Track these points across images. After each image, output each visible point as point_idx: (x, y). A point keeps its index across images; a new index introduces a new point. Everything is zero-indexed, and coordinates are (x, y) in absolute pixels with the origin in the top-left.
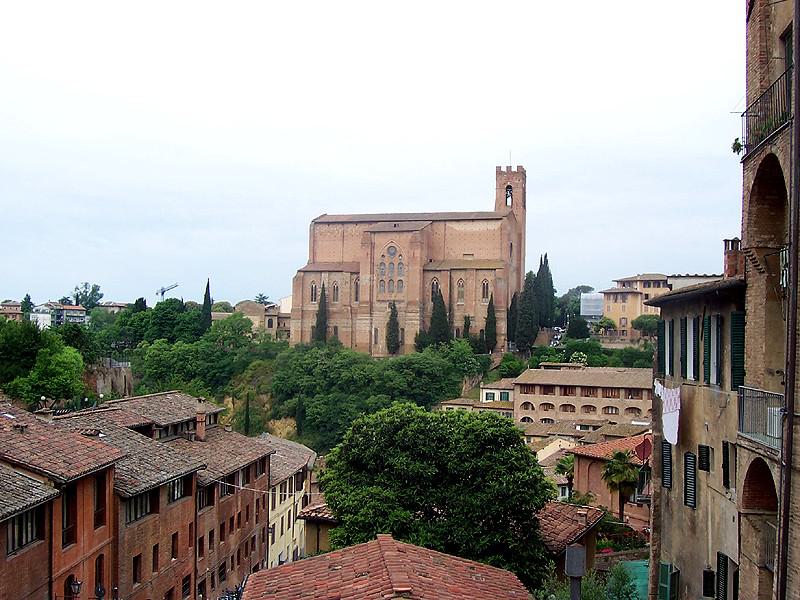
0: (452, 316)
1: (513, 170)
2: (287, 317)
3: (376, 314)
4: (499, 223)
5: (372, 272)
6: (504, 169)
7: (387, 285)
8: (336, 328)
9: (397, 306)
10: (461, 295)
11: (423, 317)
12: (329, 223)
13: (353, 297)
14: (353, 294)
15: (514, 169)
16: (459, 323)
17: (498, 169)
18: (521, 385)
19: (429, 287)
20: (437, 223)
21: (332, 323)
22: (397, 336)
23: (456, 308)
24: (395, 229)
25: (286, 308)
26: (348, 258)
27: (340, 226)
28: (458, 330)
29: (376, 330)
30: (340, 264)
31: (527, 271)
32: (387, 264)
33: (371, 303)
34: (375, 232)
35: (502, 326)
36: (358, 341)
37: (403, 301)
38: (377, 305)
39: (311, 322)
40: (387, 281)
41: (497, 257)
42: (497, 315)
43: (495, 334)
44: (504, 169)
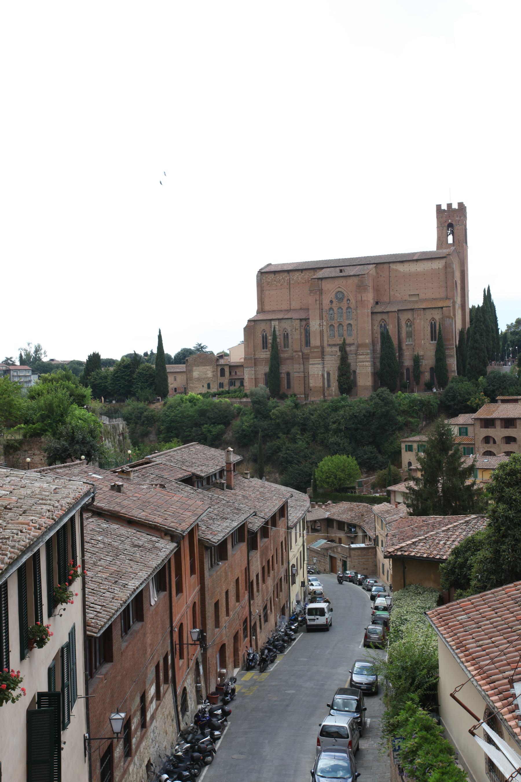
0: (401, 355)
1: (453, 207)
2: (240, 366)
3: (327, 358)
4: (443, 262)
5: (321, 318)
6: (444, 207)
7: (336, 329)
8: (288, 374)
9: (348, 349)
10: (410, 335)
11: (374, 358)
12: (275, 272)
13: (303, 343)
14: (303, 340)
15: (455, 206)
16: (408, 362)
17: (439, 207)
18: (481, 420)
19: (377, 329)
20: (382, 266)
21: (284, 369)
22: (349, 378)
23: (404, 347)
24: (342, 274)
25: (238, 358)
26: (295, 305)
27: (286, 274)
28: (408, 370)
29: (328, 374)
30: (288, 311)
31: (470, 307)
32: (335, 309)
33: (323, 348)
34: (321, 279)
35: (452, 363)
36: (311, 385)
37: (353, 344)
38: (328, 349)
39: (264, 369)
40: (336, 325)
41: (443, 295)
42: (447, 352)
43: (447, 371)
44: (444, 207)
